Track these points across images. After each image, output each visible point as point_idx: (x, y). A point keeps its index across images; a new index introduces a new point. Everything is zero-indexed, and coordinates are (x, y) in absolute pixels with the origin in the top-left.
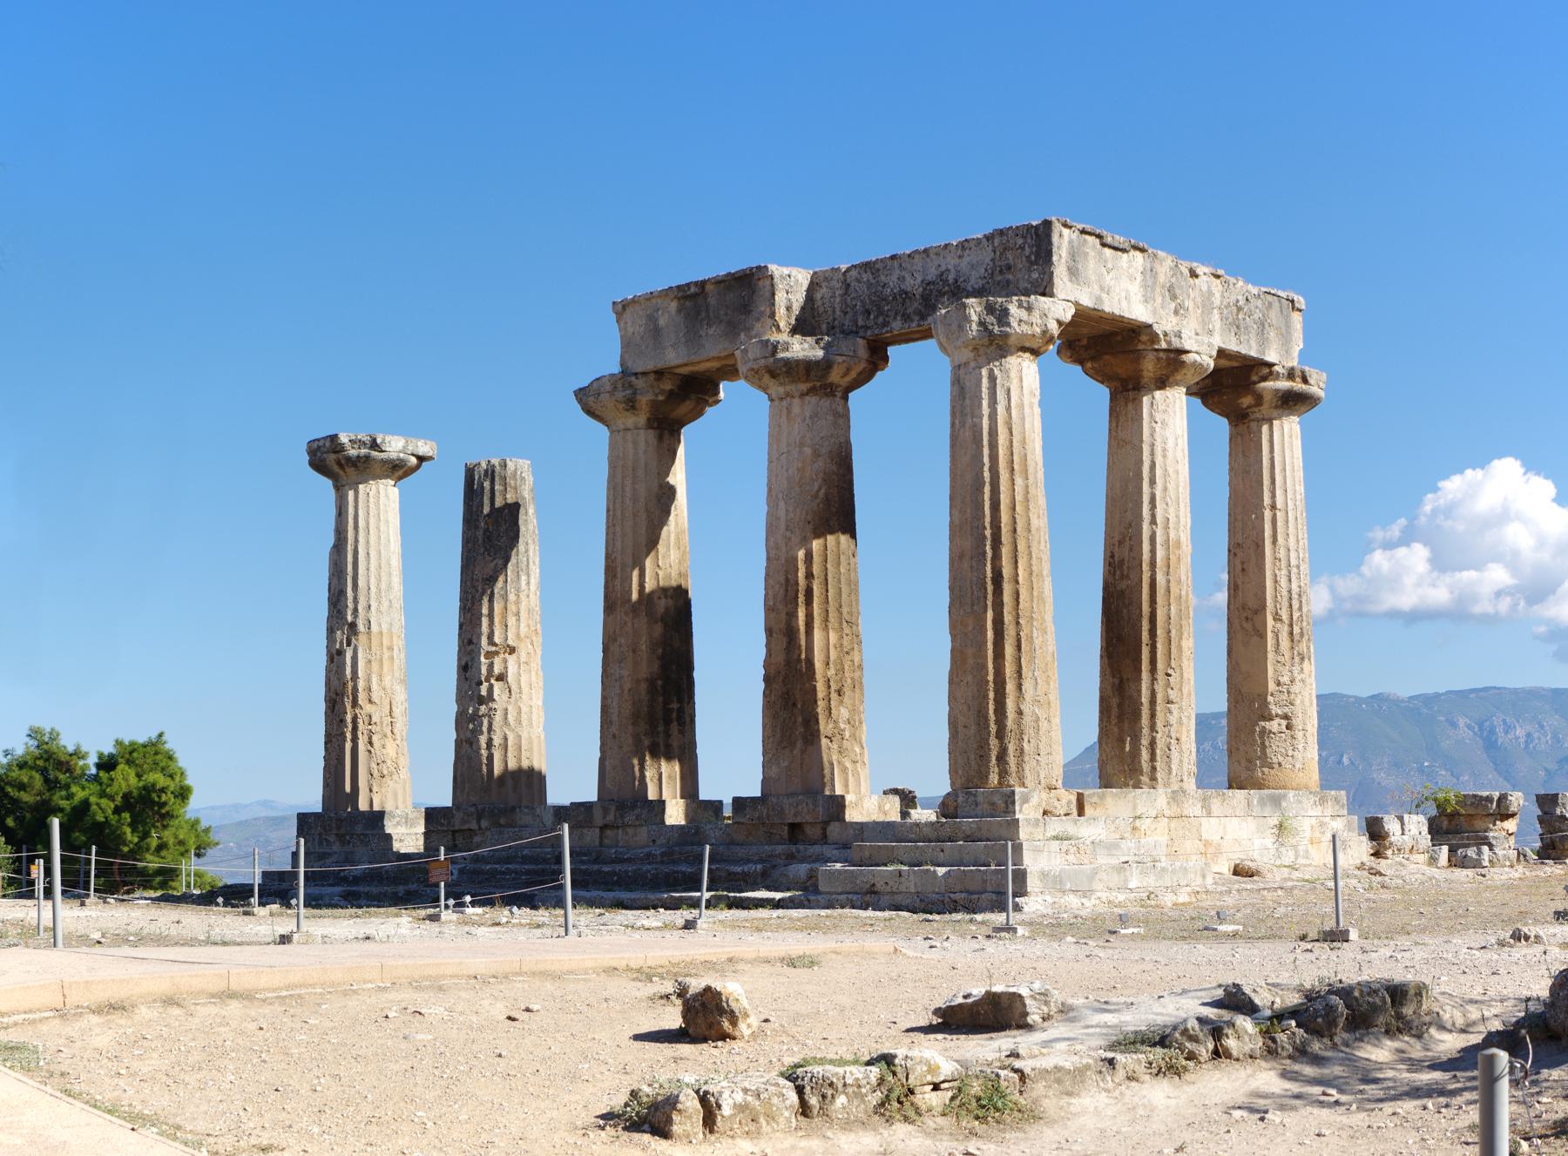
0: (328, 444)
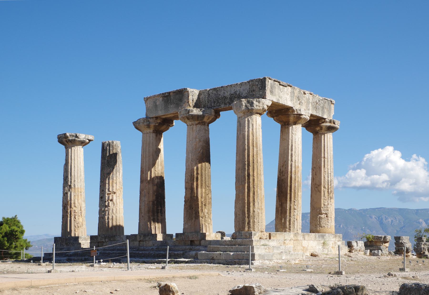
0: (63, 136)
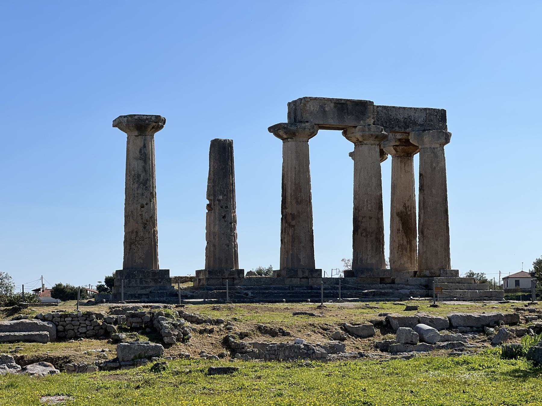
0: (153, 118)
